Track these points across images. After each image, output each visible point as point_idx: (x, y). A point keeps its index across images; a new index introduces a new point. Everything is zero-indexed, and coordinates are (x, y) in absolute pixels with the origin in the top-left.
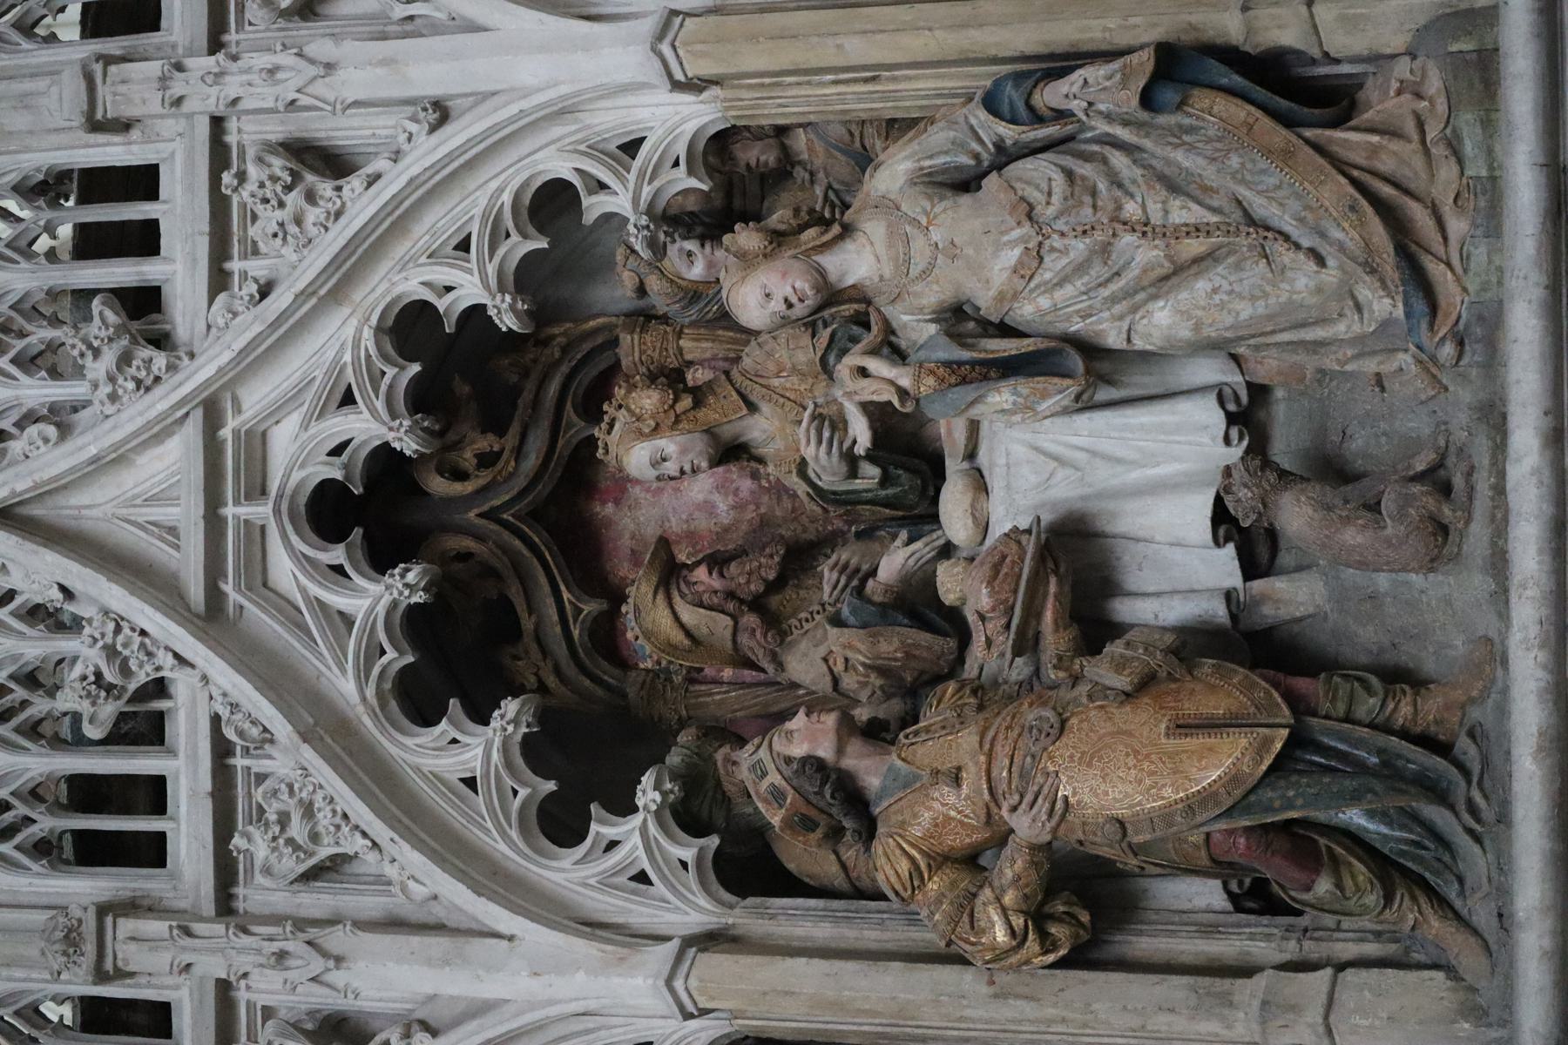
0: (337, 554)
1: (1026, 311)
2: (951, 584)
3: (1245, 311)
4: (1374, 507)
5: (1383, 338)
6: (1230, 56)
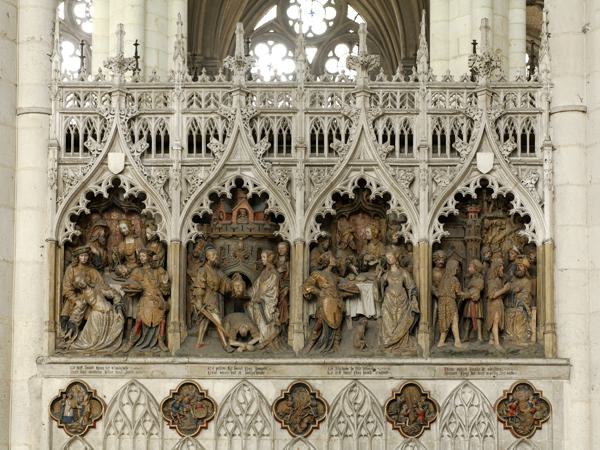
0: (356, 184)
1: (388, 295)
2: (351, 276)
3: (386, 323)
4: (362, 339)
5: (381, 341)
6: (419, 320)
